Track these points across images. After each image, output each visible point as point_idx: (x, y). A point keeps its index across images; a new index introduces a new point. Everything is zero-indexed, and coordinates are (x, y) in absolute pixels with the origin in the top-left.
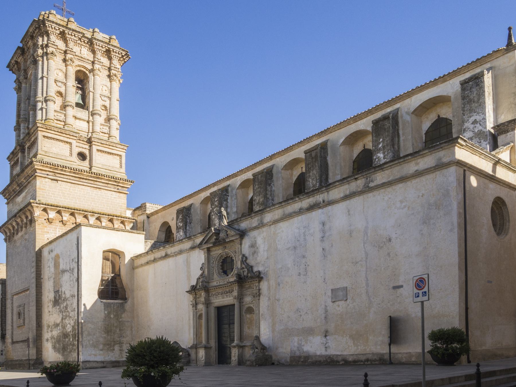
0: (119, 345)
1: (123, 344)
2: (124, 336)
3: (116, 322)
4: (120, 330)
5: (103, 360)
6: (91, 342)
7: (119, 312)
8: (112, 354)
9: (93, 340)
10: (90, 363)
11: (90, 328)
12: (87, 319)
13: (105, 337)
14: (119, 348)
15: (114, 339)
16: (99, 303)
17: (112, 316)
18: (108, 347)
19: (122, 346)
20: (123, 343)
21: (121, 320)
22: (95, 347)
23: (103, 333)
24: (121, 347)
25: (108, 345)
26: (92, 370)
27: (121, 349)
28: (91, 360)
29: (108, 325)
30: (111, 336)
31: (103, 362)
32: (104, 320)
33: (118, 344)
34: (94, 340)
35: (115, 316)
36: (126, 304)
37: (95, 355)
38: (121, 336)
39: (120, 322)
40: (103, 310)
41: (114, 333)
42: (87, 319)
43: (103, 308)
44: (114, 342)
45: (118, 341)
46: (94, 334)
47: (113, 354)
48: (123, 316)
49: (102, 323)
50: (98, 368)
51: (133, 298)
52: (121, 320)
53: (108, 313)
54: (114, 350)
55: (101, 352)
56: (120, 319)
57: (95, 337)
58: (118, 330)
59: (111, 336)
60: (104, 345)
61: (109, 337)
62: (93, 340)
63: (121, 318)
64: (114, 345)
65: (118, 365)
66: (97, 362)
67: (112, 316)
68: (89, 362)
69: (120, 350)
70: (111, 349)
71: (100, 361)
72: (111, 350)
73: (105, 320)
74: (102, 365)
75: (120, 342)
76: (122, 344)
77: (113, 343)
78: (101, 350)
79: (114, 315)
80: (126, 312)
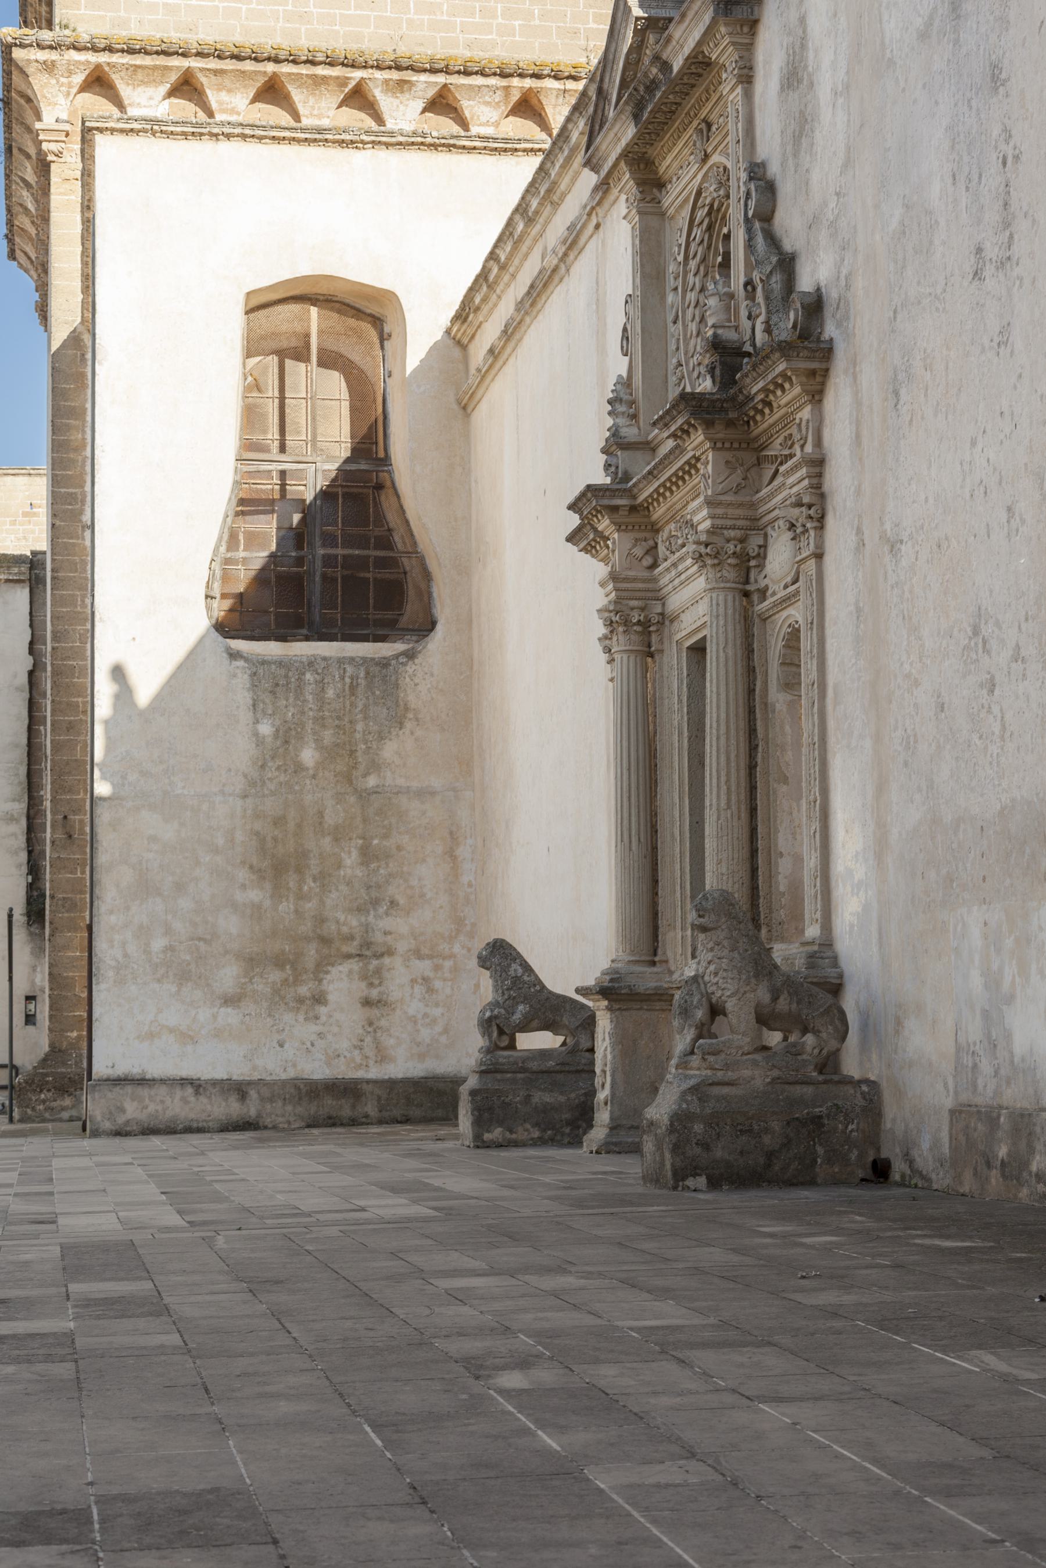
0: (354, 965)
1: (387, 960)
2: (393, 903)
3: (339, 798)
4: (367, 855)
5: (239, 1071)
6: (158, 944)
7: (360, 727)
8: (305, 1031)
9: (168, 931)
10: (144, 1092)
11: (153, 839)
12: (132, 777)
13: (257, 907)
14: (360, 988)
15: (320, 920)
16: (216, 664)
17: (308, 756)
18: (275, 976)
19: (378, 971)
20: (390, 952)
21: (372, 781)
22: (184, 977)
23: (243, 875)
24: (373, 977)
25: (279, 962)
26: (156, 1141)
27: (374, 993)
28: (154, 1070)
29: (279, 821)
30: (301, 897)
31: (239, 1089)
32: (253, 784)
33: (348, 956)
34: (178, 925)
35: (329, 754)
36: (410, 668)
37: (187, 1037)
38: (375, 902)
39: (364, 796)
40: (245, 716)
41: (323, 879)
42: (132, 777)
43: (244, 697)
44: (325, 941)
45: (352, 938)
46: (180, 888)
47: (313, 1028)
48: (389, 750)
49: (239, 803)
50: (200, 1130)
51: (467, 622)
52: (372, 781)
53: (276, 735)
54: (320, 999)
55: (230, 1016)
56: (365, 775)
57: (185, 904)
58: (351, 859)
59: (301, 897)
60: (252, 963)
61: (286, 907)
62: (168, 931)
63: (375, 766)
64: (321, 967)
65: (346, 1112)
66: (196, 1085)
67: (308, 756)
68: (142, 1081)
69: (367, 1003)
70: (303, 990)
71: (215, 1083)
72: (301, 1001)
73: (254, 786)
74: (231, 1108)
75: (367, 944)
76: (379, 956)
77: (312, 952)
78: (229, 1001)
79: (320, 747)
80: (408, 725)
